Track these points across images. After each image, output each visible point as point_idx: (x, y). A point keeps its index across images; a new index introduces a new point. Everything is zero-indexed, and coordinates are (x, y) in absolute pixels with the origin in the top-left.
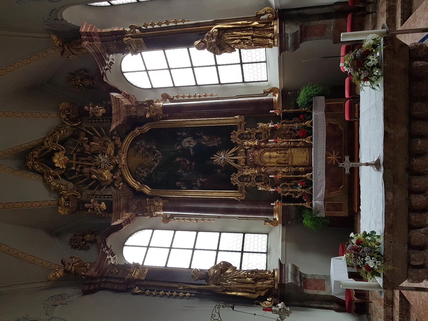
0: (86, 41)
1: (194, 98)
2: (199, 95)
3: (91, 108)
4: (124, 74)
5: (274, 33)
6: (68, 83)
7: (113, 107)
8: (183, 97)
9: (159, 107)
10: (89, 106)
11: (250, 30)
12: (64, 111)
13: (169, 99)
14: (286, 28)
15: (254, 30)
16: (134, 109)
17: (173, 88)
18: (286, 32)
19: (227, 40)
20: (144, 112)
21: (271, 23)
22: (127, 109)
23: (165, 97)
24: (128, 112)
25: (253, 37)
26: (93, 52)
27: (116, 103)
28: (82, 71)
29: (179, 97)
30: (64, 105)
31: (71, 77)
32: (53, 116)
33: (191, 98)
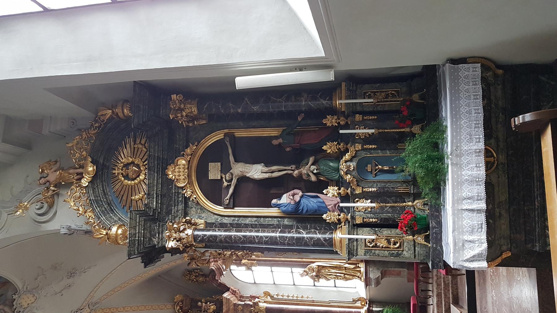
0: (213, 262)
1: (292, 298)
2: (296, 296)
3: (204, 304)
4: (231, 271)
5: (361, 273)
6: (183, 277)
7: (224, 307)
8: (283, 296)
9: (263, 308)
10: (202, 302)
11: (343, 269)
12: (178, 303)
13: (270, 296)
14: (370, 272)
15: (346, 269)
16: (241, 308)
17: (274, 285)
18: (370, 276)
19: (325, 274)
20: (249, 311)
21: (359, 264)
22: (235, 307)
23: (267, 294)
24: (235, 310)
25: (345, 274)
26: (216, 269)
27: (227, 302)
28: (198, 270)
29: (279, 296)
30: (178, 298)
31: (187, 273)
32: (168, 308)
33: (289, 298)
